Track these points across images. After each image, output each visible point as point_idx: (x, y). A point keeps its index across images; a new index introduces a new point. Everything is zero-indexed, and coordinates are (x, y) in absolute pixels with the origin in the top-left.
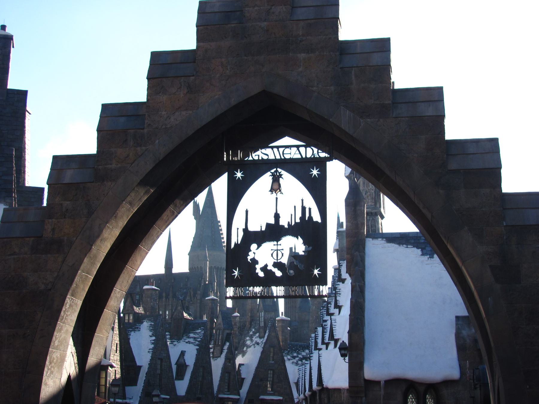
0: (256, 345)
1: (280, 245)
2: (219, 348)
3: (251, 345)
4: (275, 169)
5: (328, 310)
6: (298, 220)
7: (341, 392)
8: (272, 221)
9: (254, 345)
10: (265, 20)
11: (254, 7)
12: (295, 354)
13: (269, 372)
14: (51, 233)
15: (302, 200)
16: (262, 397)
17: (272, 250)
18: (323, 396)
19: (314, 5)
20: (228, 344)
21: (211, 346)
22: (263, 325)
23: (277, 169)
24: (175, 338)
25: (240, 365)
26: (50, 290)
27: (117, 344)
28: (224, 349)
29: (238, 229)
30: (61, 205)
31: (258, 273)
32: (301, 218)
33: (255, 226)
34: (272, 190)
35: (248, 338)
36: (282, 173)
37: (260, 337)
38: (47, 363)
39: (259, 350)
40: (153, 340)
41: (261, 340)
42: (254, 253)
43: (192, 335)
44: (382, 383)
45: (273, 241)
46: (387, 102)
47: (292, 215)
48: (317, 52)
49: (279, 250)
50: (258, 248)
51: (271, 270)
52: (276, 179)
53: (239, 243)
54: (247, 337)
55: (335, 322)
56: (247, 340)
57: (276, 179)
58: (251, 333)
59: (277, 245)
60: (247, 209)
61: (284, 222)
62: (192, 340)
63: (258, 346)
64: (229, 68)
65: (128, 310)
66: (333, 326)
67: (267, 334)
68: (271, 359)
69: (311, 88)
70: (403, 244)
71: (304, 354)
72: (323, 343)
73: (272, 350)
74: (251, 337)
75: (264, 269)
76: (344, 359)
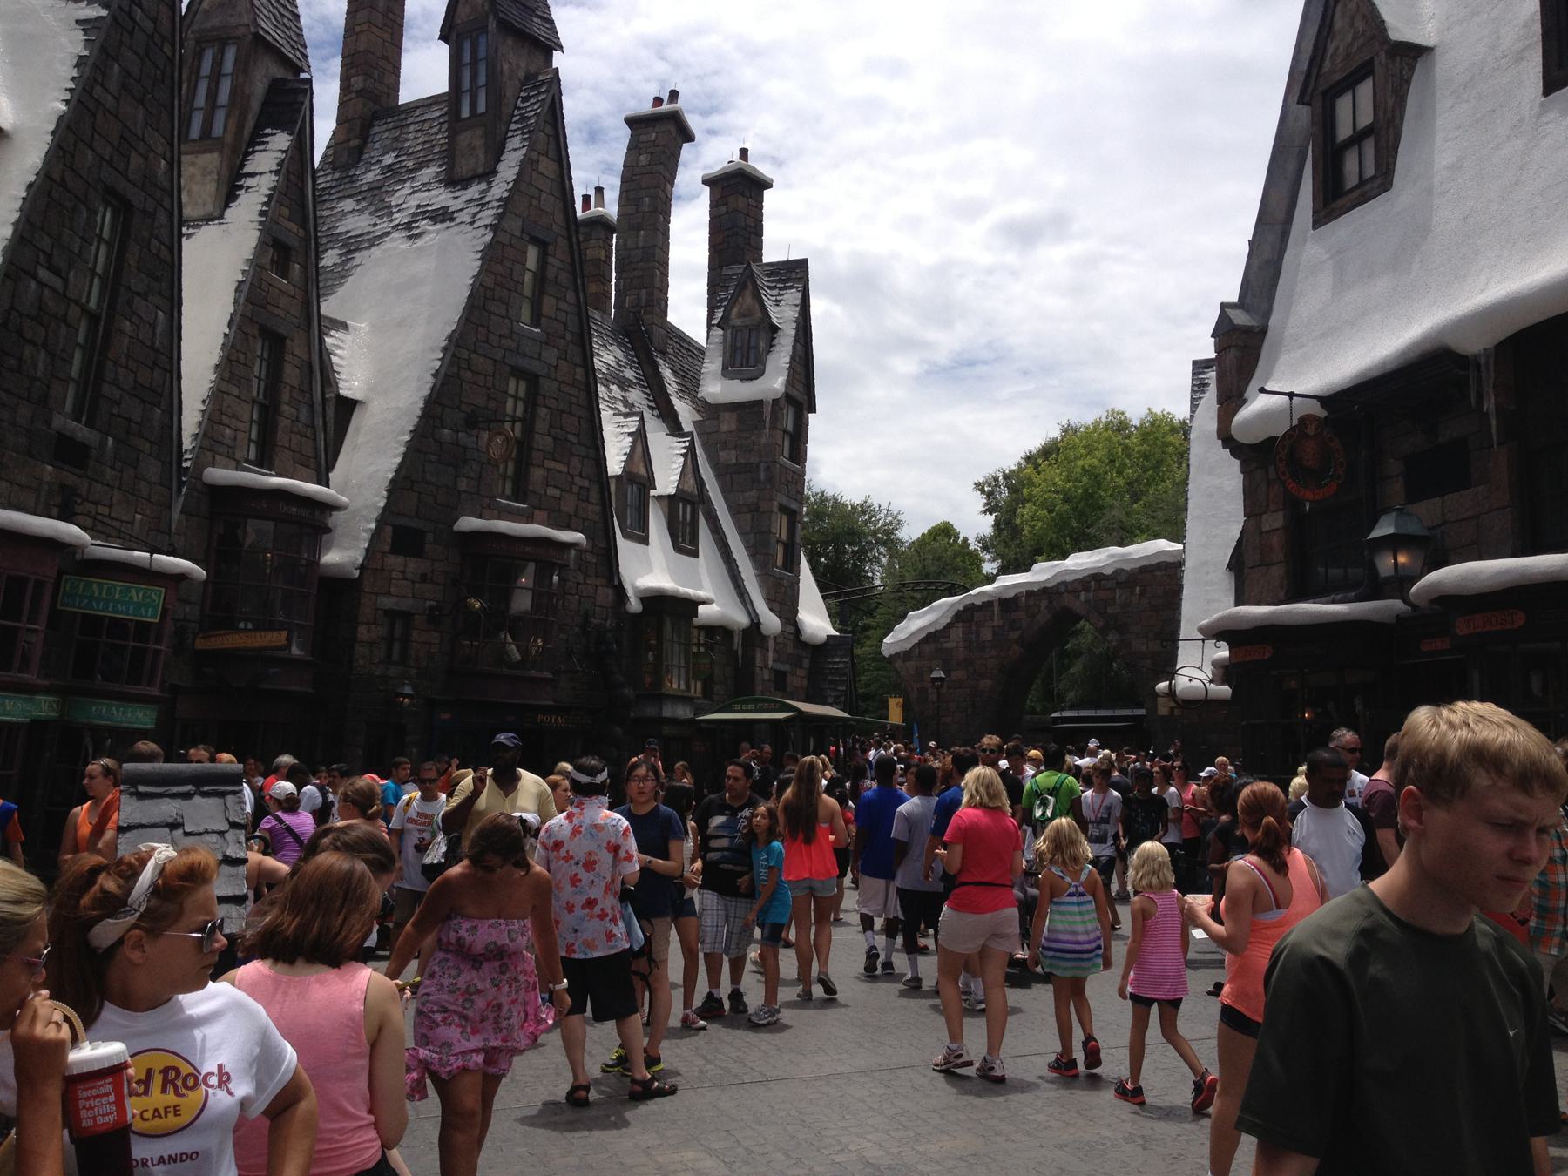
2: (211, 160)
13: (512, 384)
16: (468, 523)
22: (482, 108)
28: (246, 170)
41: (474, 191)
56: (345, 214)
58: (372, 176)
63: (448, 224)
68: (526, 313)
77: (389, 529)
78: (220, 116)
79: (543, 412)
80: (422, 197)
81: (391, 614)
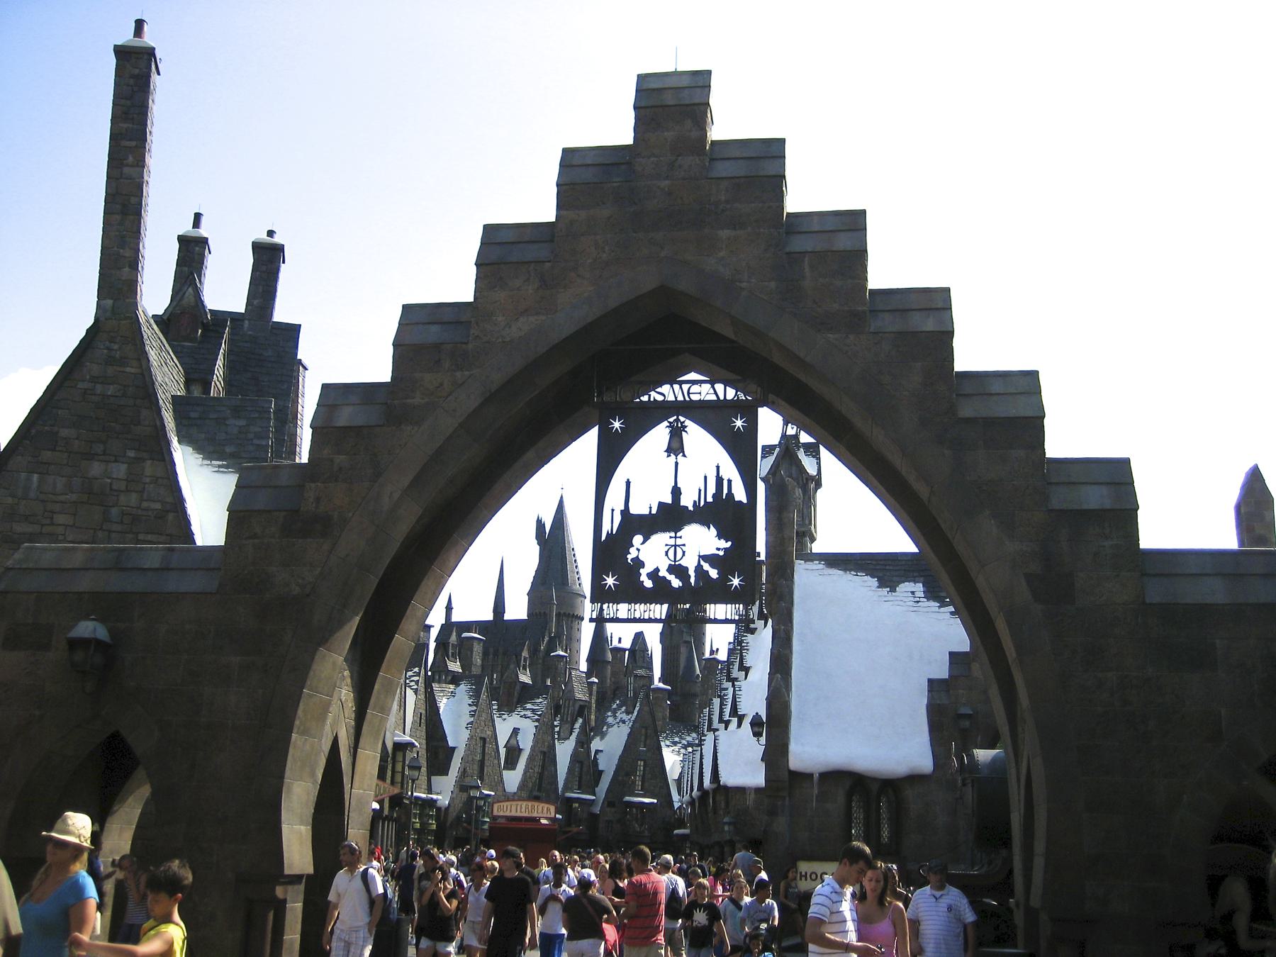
0: (621, 723)
1: (681, 537)
3: (614, 723)
4: (675, 417)
5: (729, 673)
6: (710, 499)
7: (745, 793)
8: (668, 500)
9: (618, 723)
10: (667, 178)
11: (649, 157)
12: (677, 739)
13: (639, 762)
14: (314, 505)
15: (718, 467)
16: (627, 798)
17: (667, 545)
18: (718, 798)
19: (745, 155)
20: (580, 720)
21: (555, 723)
23: (678, 417)
24: (506, 710)
25: (597, 752)
26: (308, 595)
27: (421, 714)
29: (613, 510)
30: (332, 461)
31: (643, 582)
32: (714, 496)
33: (639, 507)
34: (670, 451)
35: (609, 714)
36: (686, 424)
37: (628, 713)
38: (300, 712)
39: (625, 730)
40: (473, 711)
41: (629, 717)
42: (638, 550)
43: (529, 706)
44: (816, 776)
45: (669, 532)
46: (860, 309)
47: (700, 490)
48: (749, 228)
49: (679, 546)
50: (643, 543)
51: (664, 577)
52: (677, 434)
53: (614, 533)
54: (608, 712)
55: (740, 690)
57: (677, 434)
58: (615, 706)
59: (676, 537)
60: (628, 480)
61: (687, 501)
62: (529, 713)
64: (607, 248)
65: (439, 667)
66: (737, 696)
67: (637, 709)
69: (738, 284)
70: (850, 570)
71: (689, 739)
72: (721, 720)
73: (643, 730)
74: (614, 712)
75: (654, 575)
76: (758, 741)
77: (606, 803)
78: (569, 716)
79: (648, 769)
80: (621, 716)
81: (607, 821)
